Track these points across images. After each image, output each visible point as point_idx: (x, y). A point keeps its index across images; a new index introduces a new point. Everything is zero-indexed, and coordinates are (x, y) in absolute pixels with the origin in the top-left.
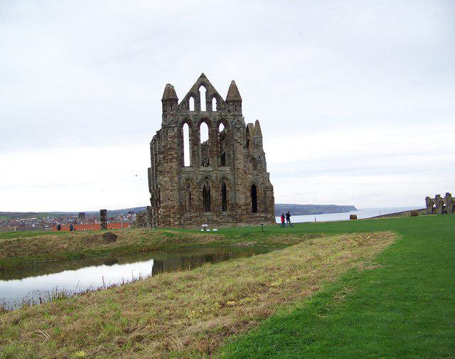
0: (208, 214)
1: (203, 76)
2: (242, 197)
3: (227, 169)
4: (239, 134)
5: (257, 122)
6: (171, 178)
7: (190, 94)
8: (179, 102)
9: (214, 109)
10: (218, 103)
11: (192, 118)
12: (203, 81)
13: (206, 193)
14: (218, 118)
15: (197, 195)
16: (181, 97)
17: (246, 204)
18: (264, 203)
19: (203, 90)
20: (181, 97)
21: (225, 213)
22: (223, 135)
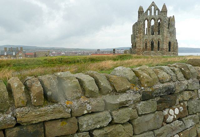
0: (152, 51)
1: (153, 2)
2: (166, 46)
3: (160, 36)
4: (165, 24)
5: (173, 16)
6: (140, 39)
7: (148, 9)
8: (144, 12)
9: (157, 14)
10: (158, 12)
11: (148, 18)
12: (153, 4)
13: (152, 44)
14: (158, 18)
15: (149, 45)
16: (145, 11)
17: (166, 49)
18: (174, 48)
19: (153, 7)
20: (145, 11)
21: (158, 51)
22: (159, 24)
